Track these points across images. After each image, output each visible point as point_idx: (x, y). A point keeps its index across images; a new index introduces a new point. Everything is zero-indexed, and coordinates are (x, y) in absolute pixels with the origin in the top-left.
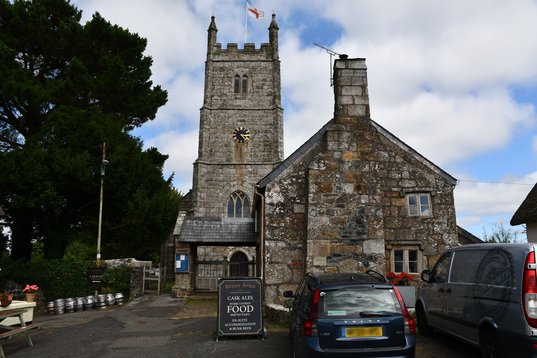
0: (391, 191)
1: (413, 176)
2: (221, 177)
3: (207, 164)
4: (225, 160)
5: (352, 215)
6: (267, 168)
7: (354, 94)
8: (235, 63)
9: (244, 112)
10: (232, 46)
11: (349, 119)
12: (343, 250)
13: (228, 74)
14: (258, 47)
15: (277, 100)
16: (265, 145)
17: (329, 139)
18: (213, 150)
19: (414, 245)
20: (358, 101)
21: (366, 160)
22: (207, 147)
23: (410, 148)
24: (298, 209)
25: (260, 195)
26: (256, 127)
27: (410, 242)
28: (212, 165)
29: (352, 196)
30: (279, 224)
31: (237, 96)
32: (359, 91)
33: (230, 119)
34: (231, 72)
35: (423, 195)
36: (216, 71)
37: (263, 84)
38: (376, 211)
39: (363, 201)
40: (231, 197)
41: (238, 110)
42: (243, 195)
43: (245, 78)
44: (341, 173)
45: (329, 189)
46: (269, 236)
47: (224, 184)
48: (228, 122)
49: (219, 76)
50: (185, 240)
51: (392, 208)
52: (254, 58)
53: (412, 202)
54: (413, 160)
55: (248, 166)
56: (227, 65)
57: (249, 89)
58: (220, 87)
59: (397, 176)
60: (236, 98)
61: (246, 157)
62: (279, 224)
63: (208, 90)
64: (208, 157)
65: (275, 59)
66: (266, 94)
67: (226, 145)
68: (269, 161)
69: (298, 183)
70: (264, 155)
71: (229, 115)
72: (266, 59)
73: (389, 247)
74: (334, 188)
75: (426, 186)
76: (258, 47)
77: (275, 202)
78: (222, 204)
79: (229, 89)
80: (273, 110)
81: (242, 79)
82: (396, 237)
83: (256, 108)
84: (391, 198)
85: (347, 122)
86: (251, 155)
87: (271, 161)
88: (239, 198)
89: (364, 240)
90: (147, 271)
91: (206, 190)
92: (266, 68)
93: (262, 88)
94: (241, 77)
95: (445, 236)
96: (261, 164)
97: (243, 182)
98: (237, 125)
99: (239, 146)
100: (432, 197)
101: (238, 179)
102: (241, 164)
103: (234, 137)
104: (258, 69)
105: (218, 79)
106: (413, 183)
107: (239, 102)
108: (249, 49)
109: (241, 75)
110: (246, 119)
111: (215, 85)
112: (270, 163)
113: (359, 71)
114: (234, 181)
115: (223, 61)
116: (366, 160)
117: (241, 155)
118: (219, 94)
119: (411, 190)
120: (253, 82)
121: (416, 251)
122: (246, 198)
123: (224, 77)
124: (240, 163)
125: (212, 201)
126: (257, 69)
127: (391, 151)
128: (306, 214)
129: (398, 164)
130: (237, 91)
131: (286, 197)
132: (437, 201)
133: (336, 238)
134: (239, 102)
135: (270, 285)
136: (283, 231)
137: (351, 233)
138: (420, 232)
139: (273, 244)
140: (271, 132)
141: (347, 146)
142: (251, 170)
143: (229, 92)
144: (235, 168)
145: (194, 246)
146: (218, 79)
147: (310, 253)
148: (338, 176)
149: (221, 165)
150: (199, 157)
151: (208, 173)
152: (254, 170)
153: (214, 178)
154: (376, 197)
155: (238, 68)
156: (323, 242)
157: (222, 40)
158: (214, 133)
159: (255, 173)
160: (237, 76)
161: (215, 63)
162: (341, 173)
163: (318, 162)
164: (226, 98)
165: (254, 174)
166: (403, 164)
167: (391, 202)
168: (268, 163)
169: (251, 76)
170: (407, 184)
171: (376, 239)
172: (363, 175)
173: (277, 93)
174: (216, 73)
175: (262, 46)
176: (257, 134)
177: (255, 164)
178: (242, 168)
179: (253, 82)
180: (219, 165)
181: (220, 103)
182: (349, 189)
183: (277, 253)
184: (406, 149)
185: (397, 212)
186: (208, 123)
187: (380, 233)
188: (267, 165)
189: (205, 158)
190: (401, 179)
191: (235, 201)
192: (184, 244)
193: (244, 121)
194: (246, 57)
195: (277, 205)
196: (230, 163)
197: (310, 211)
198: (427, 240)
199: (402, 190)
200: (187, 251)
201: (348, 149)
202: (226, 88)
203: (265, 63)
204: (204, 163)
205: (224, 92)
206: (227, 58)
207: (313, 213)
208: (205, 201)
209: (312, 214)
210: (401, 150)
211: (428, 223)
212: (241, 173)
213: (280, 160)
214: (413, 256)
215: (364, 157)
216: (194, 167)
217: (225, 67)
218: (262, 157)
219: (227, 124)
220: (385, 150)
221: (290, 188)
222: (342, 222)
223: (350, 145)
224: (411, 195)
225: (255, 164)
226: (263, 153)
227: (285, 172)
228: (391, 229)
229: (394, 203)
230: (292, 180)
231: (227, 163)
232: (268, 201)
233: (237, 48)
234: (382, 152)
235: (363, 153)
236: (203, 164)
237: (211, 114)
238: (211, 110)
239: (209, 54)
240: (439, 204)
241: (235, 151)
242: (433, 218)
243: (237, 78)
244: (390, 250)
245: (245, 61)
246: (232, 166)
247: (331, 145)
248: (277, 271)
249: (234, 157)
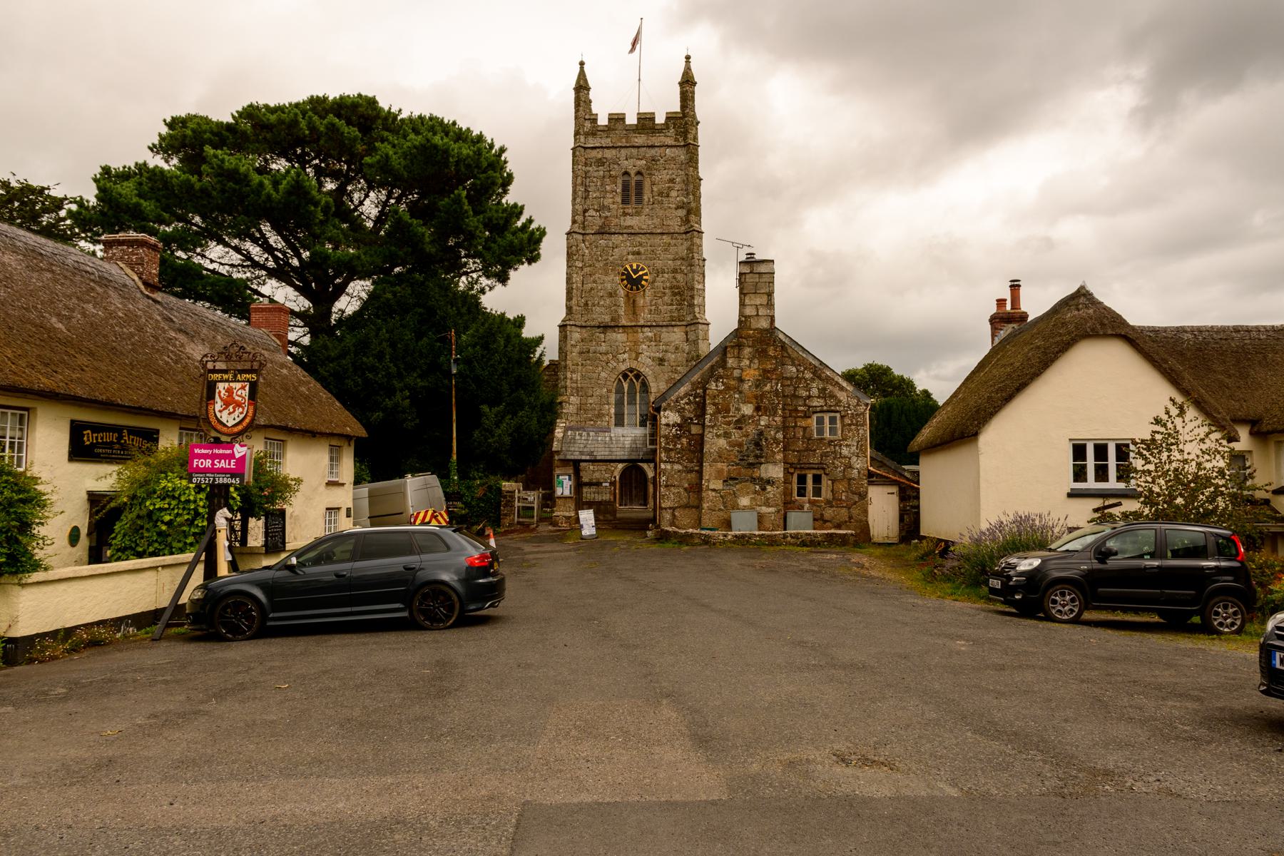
0: (796, 410)
1: (823, 393)
2: (604, 348)
4: (609, 320)
5: (750, 438)
7: (758, 303)
8: (622, 150)
9: (638, 239)
10: (617, 119)
11: (751, 332)
12: (739, 474)
13: (610, 171)
14: (660, 120)
15: (692, 217)
16: (674, 294)
17: (729, 355)
18: (589, 302)
19: (818, 469)
20: (762, 312)
21: (768, 378)
22: (580, 299)
23: (821, 363)
24: (695, 430)
25: (656, 413)
26: (659, 264)
27: (814, 466)
29: (751, 417)
30: (675, 445)
31: (626, 211)
32: (764, 300)
33: (615, 250)
34: (615, 166)
35: (833, 414)
36: (591, 166)
37: (669, 187)
38: (776, 433)
39: (762, 423)
40: (620, 380)
41: (628, 234)
42: (638, 376)
43: (639, 178)
44: (741, 392)
45: (728, 411)
46: (665, 459)
47: (608, 358)
48: (612, 255)
49: (596, 174)
51: (797, 429)
52: (656, 140)
53: (820, 421)
54: (823, 375)
55: (646, 329)
56: (609, 154)
57: (645, 198)
58: (597, 194)
59: (805, 394)
60: (625, 214)
62: (675, 445)
63: (578, 200)
65: (690, 144)
66: (674, 206)
67: (610, 295)
68: (680, 321)
69: (696, 402)
70: (671, 311)
71: (613, 243)
72: (674, 143)
73: (792, 470)
74: (733, 409)
75: (836, 405)
76: (660, 120)
77: (671, 423)
78: (605, 390)
79: (613, 200)
80: (686, 233)
81: (634, 178)
82: (799, 460)
83: (659, 231)
84: (795, 418)
85: (749, 336)
86: (651, 310)
87: (683, 321)
88: (631, 380)
89: (761, 463)
91: (580, 368)
92: (673, 159)
93: (668, 196)
94: (633, 175)
95: (854, 459)
96: (667, 326)
97: (638, 354)
98: (627, 260)
99: (630, 296)
100: (842, 417)
101: (630, 349)
102: (635, 326)
103: (622, 280)
104: (662, 161)
105: (595, 179)
106: (821, 402)
107: (629, 221)
108: (646, 121)
109: (632, 173)
110: (642, 250)
111: (589, 191)
113: (766, 275)
114: (624, 353)
115: (602, 147)
116: (768, 378)
117: (634, 310)
118: (596, 207)
119: (818, 409)
120: (653, 184)
121: (821, 475)
122: (643, 379)
123: (604, 177)
124: (633, 324)
125: (589, 386)
126: (659, 160)
127: (800, 365)
128: (702, 436)
129: (806, 380)
130: (625, 201)
131: (683, 417)
132: (847, 421)
133: (733, 461)
134: (629, 221)
135: (665, 509)
136: (679, 453)
137: (748, 456)
138: (825, 455)
139: (669, 467)
140: (682, 272)
141: (748, 363)
142: (650, 334)
143: (614, 203)
145: (576, 464)
146: (595, 179)
147: (706, 477)
148: (737, 396)
150: (567, 314)
151: (582, 341)
153: (592, 349)
154: (776, 419)
155: (627, 159)
156: (719, 465)
157: (602, 110)
158: (590, 275)
159: (657, 340)
160: (626, 173)
161: (588, 151)
162: (741, 392)
163: (717, 381)
164: (608, 214)
165: (656, 341)
166: (812, 380)
167: (796, 423)
169: (650, 174)
170: (816, 403)
171: (775, 463)
172: (763, 396)
173: (693, 205)
174: (591, 169)
175: (667, 118)
176: (661, 275)
178: (637, 332)
179: (653, 184)
181: (599, 222)
182: (748, 410)
183: (673, 476)
184: (817, 364)
185: (801, 433)
186: (581, 257)
187: (779, 457)
189: (577, 317)
190: (809, 397)
191: (626, 386)
192: (565, 462)
193: (638, 253)
194: (640, 140)
195: (674, 426)
197: (706, 433)
198: (833, 463)
199: (809, 410)
201: (750, 367)
202: (608, 195)
203: (673, 150)
204: (575, 325)
205: (606, 204)
206: (606, 142)
207: (710, 435)
208: (579, 385)
209: (708, 437)
210: (810, 364)
211: (835, 446)
214: (817, 479)
215: (766, 375)
216: (560, 332)
217: (606, 158)
219: (611, 259)
220: (793, 364)
221: (686, 407)
222: (740, 445)
223: (751, 362)
224: (819, 415)
226: (670, 307)
227: (683, 390)
228: (794, 451)
229: (799, 424)
230: (689, 399)
231: (613, 324)
232: (664, 421)
233: (624, 122)
234: (789, 367)
235: (765, 371)
237: (584, 241)
238: (583, 234)
239: (577, 133)
240: (850, 425)
241: (625, 303)
242: (840, 440)
243: (626, 178)
244: (792, 474)
245: (638, 147)
247: (731, 362)
248: (673, 494)
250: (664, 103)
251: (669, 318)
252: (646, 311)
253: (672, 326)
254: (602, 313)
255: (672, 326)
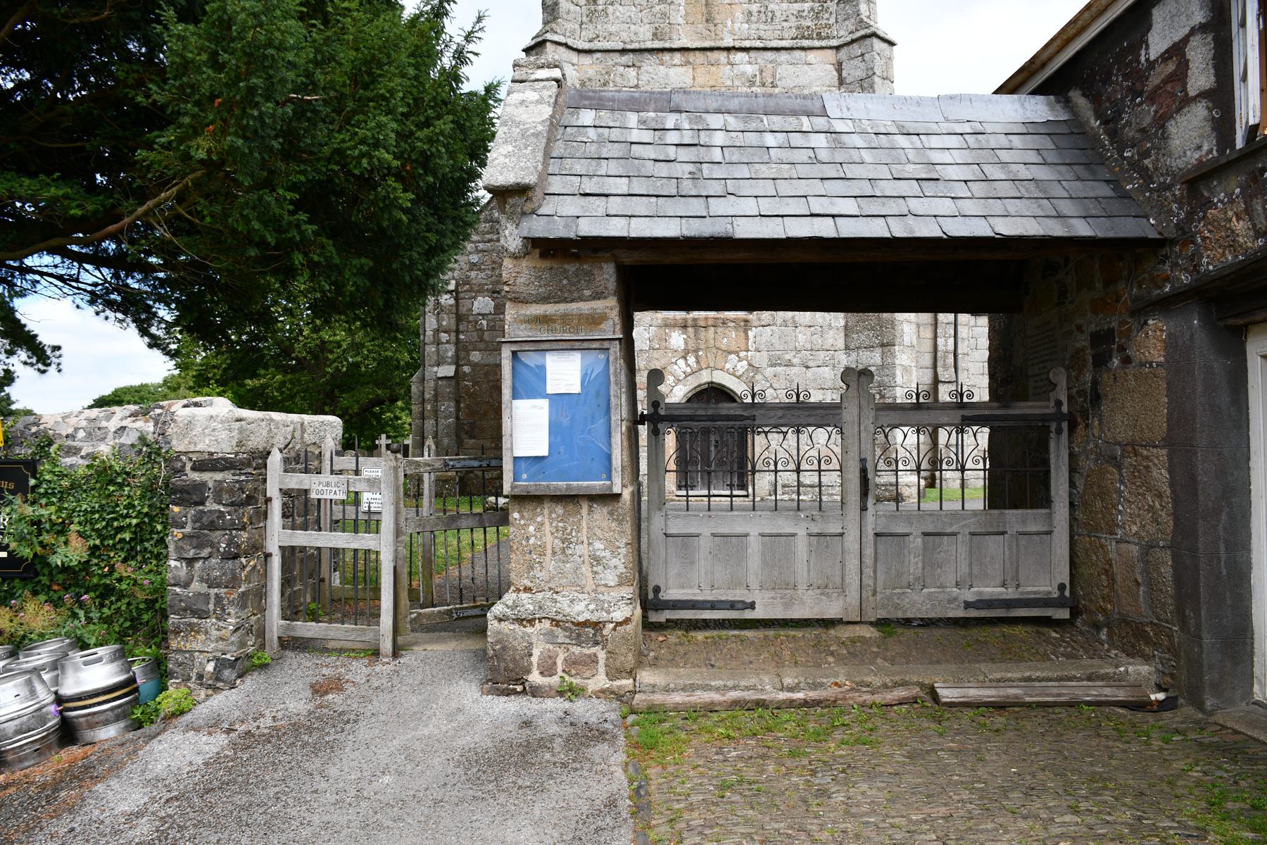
3: (579, 51)
4: (649, 35)
6: (813, 61)
28: (598, 55)
50: (587, 228)
55: (739, 57)
61: (729, 23)
64: (582, 23)
68: (820, 37)
70: (799, 15)
86: (750, 13)
87: (828, 38)
90: (297, 481)
96: (792, 49)
102: (712, 49)
112: (824, 43)
117: (709, 13)
124: (707, 44)
144: (688, 63)
149: (633, 51)
150: (545, 23)
152: (761, 71)
168: (817, 43)
177: (765, 49)
178: (717, 64)
180: (623, 51)
188: (814, 52)
189: (569, 26)
196: (667, 45)
200: (595, 320)
204: (566, 45)
212: (712, 83)
213: (869, 26)
218: (793, 22)
225: (765, 49)
231: (657, 44)
236: (562, 49)
246: (678, 56)
249: (681, 21)
251: (793, 32)
252: (739, 15)
253: (803, 49)
254: (630, 21)
255: (803, 49)
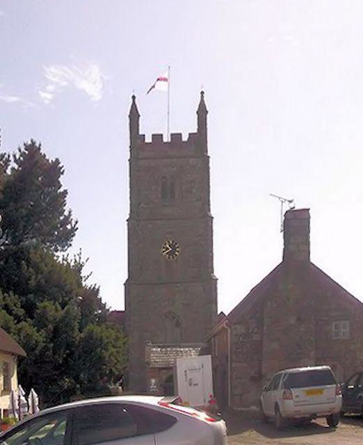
10: (157, 137)
14: (185, 138)
57: (177, 194)
60: (164, 206)
108: (176, 137)
157: (147, 130)
238: (138, 220)
250: (188, 127)
